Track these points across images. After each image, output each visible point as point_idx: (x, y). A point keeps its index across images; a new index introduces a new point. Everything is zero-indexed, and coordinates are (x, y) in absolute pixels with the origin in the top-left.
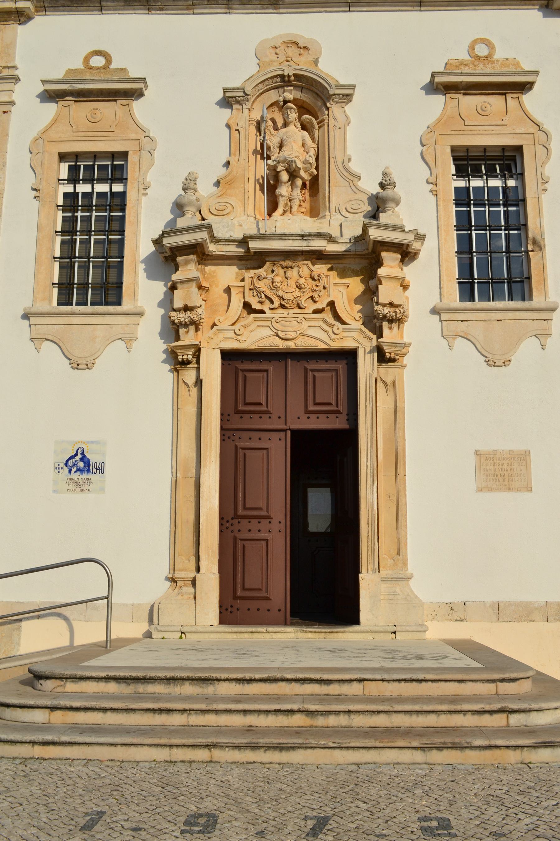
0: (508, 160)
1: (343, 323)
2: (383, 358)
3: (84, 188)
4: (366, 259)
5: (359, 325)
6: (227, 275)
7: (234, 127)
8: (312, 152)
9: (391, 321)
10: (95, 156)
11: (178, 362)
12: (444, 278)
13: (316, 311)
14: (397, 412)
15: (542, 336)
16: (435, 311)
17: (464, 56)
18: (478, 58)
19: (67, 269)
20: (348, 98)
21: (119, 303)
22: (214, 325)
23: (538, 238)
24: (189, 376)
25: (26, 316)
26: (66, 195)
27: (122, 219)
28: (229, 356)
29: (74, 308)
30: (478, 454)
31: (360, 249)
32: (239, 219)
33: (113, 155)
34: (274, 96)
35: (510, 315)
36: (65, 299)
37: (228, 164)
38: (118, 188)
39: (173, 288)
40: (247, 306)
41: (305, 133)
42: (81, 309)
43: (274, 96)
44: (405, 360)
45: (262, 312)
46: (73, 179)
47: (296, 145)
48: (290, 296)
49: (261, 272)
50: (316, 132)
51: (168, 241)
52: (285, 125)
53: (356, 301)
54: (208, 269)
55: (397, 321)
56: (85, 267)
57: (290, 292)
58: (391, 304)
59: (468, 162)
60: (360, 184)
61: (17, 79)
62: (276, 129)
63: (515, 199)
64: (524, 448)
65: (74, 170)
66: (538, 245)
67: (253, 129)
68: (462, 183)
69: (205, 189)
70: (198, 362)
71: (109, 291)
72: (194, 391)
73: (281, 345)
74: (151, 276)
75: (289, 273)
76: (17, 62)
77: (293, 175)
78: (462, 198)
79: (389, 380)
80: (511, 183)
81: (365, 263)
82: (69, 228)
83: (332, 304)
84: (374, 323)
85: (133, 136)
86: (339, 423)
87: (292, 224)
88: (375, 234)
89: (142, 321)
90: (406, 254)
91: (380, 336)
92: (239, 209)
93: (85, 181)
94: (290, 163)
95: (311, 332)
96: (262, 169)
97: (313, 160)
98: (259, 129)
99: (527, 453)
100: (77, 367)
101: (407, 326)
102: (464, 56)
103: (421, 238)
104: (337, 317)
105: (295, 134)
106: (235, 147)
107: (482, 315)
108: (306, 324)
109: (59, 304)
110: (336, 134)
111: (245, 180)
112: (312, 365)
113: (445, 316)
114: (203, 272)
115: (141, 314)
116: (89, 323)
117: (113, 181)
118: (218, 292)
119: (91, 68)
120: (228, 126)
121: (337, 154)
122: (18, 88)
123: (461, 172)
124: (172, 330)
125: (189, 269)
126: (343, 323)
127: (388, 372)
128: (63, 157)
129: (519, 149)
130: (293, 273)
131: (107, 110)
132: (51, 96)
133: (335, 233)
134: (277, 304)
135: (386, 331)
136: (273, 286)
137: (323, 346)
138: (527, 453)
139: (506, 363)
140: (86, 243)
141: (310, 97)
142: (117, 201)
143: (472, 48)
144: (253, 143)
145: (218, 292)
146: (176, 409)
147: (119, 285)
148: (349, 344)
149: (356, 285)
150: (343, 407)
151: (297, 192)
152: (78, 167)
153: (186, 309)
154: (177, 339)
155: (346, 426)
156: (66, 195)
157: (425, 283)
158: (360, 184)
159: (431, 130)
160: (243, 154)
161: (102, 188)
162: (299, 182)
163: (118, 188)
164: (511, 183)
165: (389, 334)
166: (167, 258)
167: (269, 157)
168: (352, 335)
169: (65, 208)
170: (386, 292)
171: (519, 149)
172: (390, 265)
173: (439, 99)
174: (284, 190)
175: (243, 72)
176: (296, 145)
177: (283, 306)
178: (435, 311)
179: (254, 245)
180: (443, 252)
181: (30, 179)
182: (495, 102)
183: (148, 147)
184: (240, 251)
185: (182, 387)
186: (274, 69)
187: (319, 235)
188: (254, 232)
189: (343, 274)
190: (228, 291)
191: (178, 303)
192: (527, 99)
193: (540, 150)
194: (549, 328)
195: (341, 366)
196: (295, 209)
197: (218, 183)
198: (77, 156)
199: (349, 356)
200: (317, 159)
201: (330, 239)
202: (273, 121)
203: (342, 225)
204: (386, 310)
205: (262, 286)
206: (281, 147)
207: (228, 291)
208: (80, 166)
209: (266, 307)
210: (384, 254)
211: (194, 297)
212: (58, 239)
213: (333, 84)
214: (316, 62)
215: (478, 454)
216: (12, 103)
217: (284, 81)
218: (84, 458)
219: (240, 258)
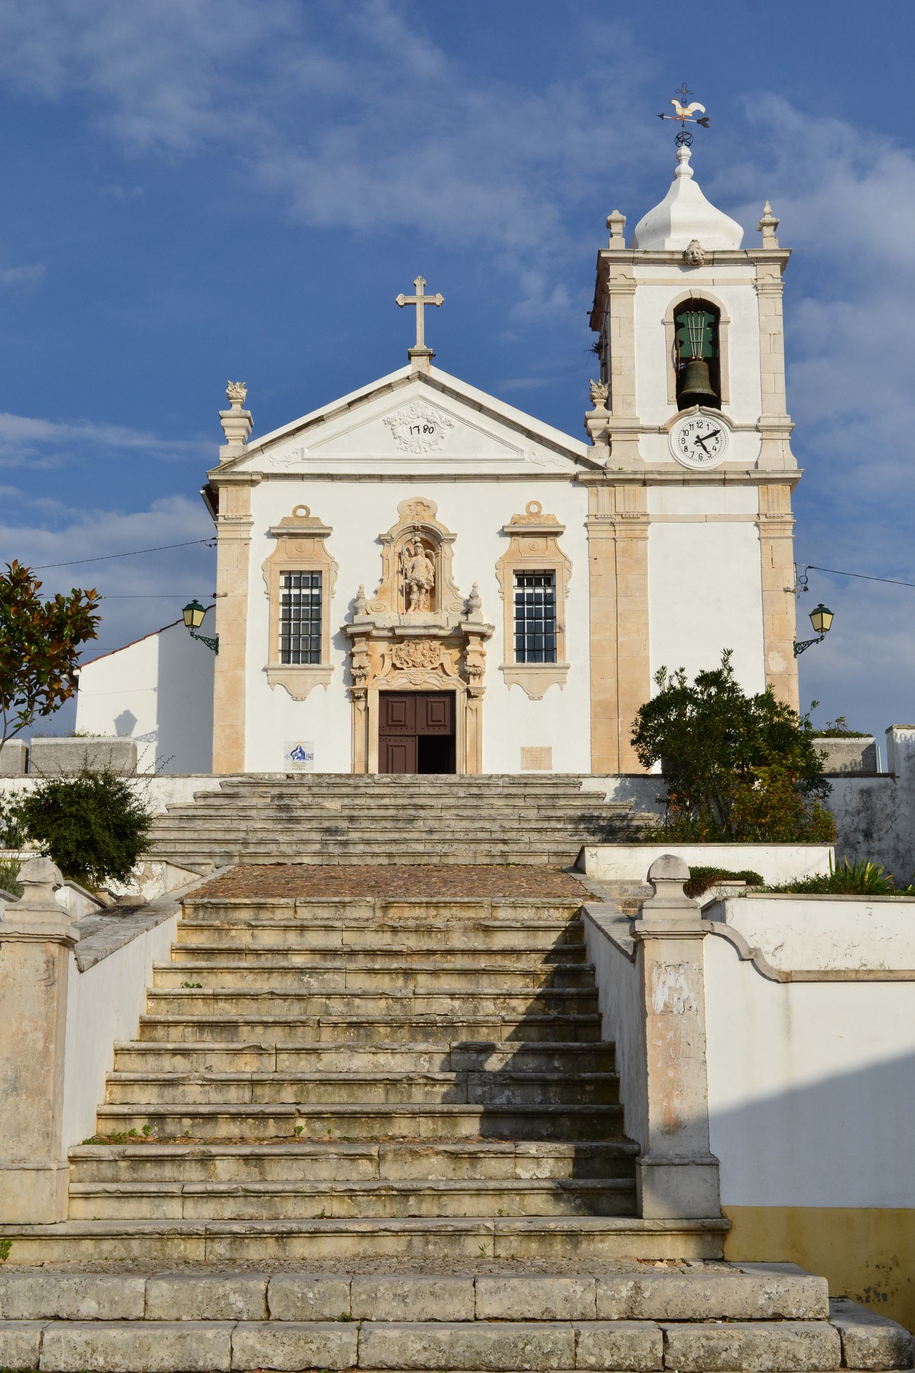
0: (547, 577)
1: (448, 675)
2: (470, 696)
3: (294, 592)
4: (460, 640)
5: (457, 676)
6: (382, 647)
7: (385, 557)
8: (432, 574)
9: (474, 675)
10: (301, 572)
11: (354, 697)
12: (507, 649)
13: (433, 669)
14: (478, 726)
15: (562, 683)
16: (501, 668)
17: (524, 513)
18: (531, 514)
19: (286, 640)
20: (453, 540)
21: (318, 662)
22: (375, 676)
23: (562, 625)
24: (361, 705)
25: (265, 670)
26: (284, 596)
27: (319, 612)
28: (382, 693)
29: (291, 665)
30: (522, 749)
31: (457, 633)
32: (389, 615)
33: (312, 572)
34: (409, 536)
35: (543, 671)
36: (286, 660)
37: (382, 580)
38: (316, 592)
39: (352, 655)
40: (394, 665)
41: (427, 560)
42: (296, 665)
43: (409, 536)
44: (483, 696)
45: (402, 669)
46: (288, 586)
47: (422, 570)
48: (418, 661)
49: (401, 646)
50: (434, 560)
51: (350, 630)
52: (416, 555)
53: (456, 663)
54: (371, 643)
55: (479, 675)
56: (297, 640)
57: (419, 659)
58: (474, 666)
59: (525, 578)
60: (459, 593)
61: (252, 523)
62: (410, 556)
63: (550, 600)
64: (546, 745)
65: (288, 580)
66: (562, 630)
67: (397, 558)
68: (520, 591)
69: (369, 595)
70: (366, 697)
71: (314, 655)
72: (364, 713)
73: (413, 688)
74: (338, 647)
75: (418, 647)
76: (251, 513)
77: (420, 587)
78: (520, 600)
79: (473, 708)
80: (549, 591)
81: (461, 640)
82: (286, 618)
83: (442, 665)
84: (465, 676)
85: (324, 561)
86: (446, 732)
87: (419, 618)
88: (465, 628)
89: (333, 673)
90: (483, 637)
91: (468, 683)
92: (389, 608)
93: (295, 587)
94: (418, 581)
95: (430, 680)
96: (402, 582)
97: (432, 579)
98: (400, 557)
99: (550, 748)
100: (296, 699)
101: (484, 677)
102: (524, 513)
103: (493, 628)
104: (445, 672)
105: (421, 560)
106: (386, 569)
107: (527, 671)
108: (427, 676)
109: (283, 662)
110: (445, 563)
111: (392, 589)
112: (431, 699)
113: (506, 671)
114: (368, 645)
115: (332, 669)
116: (301, 673)
117: (312, 588)
118: (377, 657)
119: (298, 517)
120: (382, 556)
121: (446, 575)
122: (253, 528)
123: (520, 584)
124: (352, 679)
125: (361, 646)
126: (448, 675)
127: (473, 703)
128: (282, 573)
129: (554, 570)
130: (420, 647)
131: (308, 543)
132: (272, 535)
133: (444, 624)
134: (411, 664)
135: (471, 680)
136: (409, 655)
137: (436, 689)
138: (550, 748)
139: (540, 698)
140: (297, 626)
141: (431, 540)
142: (315, 601)
143: (528, 507)
144: (397, 566)
145: (377, 657)
146: (354, 724)
147: (319, 652)
148: (451, 687)
149: (456, 654)
150: (448, 723)
151: (423, 597)
152: (290, 578)
153: (360, 668)
154: (354, 683)
155: (449, 733)
156: (284, 596)
157: (496, 652)
158: (459, 593)
159: (502, 559)
160: (391, 575)
161: (306, 592)
162: (424, 591)
163: (316, 592)
164: (549, 591)
165: (473, 682)
166: (348, 638)
167: (406, 578)
168: (452, 682)
169: (284, 604)
170: (470, 660)
171: (554, 570)
172: (474, 645)
173: (508, 540)
174: (414, 596)
175: (388, 522)
176: (422, 570)
177: (414, 666)
178: (501, 668)
179: (398, 632)
180: (506, 634)
181: (263, 587)
182: (540, 541)
183: (334, 568)
184: (390, 634)
185: (357, 712)
186: (409, 522)
187: (435, 626)
188: (397, 624)
189: (448, 647)
190: (383, 656)
191: (355, 665)
192: (559, 540)
193: (565, 572)
194: (565, 678)
195: (447, 700)
196: (421, 607)
197: (376, 592)
198: (290, 572)
199: (452, 694)
200: (434, 576)
201: (441, 628)
202: (408, 550)
203: (447, 619)
204: (471, 669)
205: (402, 654)
206: (413, 568)
207: (383, 656)
208: (294, 579)
209: (404, 666)
210: (470, 638)
211: (365, 662)
212: (281, 623)
213: (444, 532)
214: (434, 516)
215: (522, 749)
216: (250, 539)
217: (415, 529)
218: (301, 751)
219: (390, 638)
